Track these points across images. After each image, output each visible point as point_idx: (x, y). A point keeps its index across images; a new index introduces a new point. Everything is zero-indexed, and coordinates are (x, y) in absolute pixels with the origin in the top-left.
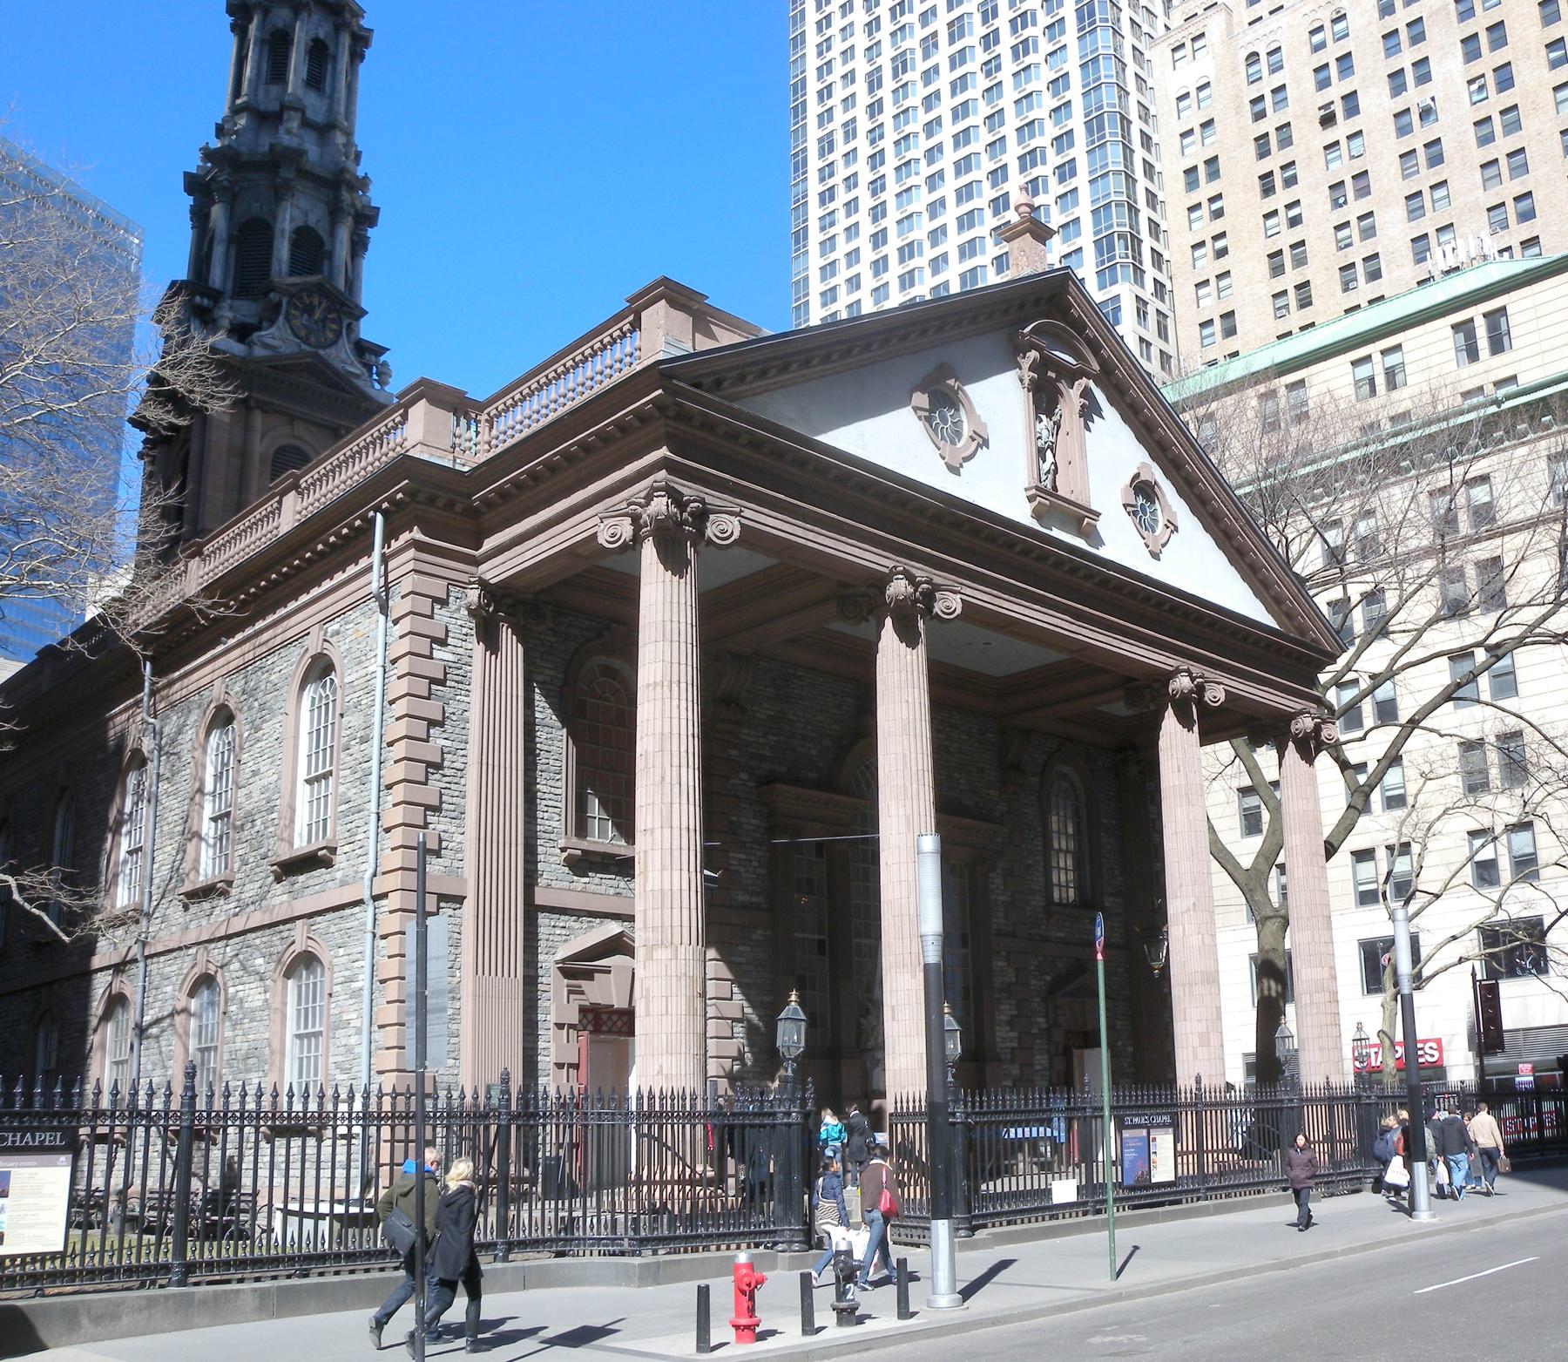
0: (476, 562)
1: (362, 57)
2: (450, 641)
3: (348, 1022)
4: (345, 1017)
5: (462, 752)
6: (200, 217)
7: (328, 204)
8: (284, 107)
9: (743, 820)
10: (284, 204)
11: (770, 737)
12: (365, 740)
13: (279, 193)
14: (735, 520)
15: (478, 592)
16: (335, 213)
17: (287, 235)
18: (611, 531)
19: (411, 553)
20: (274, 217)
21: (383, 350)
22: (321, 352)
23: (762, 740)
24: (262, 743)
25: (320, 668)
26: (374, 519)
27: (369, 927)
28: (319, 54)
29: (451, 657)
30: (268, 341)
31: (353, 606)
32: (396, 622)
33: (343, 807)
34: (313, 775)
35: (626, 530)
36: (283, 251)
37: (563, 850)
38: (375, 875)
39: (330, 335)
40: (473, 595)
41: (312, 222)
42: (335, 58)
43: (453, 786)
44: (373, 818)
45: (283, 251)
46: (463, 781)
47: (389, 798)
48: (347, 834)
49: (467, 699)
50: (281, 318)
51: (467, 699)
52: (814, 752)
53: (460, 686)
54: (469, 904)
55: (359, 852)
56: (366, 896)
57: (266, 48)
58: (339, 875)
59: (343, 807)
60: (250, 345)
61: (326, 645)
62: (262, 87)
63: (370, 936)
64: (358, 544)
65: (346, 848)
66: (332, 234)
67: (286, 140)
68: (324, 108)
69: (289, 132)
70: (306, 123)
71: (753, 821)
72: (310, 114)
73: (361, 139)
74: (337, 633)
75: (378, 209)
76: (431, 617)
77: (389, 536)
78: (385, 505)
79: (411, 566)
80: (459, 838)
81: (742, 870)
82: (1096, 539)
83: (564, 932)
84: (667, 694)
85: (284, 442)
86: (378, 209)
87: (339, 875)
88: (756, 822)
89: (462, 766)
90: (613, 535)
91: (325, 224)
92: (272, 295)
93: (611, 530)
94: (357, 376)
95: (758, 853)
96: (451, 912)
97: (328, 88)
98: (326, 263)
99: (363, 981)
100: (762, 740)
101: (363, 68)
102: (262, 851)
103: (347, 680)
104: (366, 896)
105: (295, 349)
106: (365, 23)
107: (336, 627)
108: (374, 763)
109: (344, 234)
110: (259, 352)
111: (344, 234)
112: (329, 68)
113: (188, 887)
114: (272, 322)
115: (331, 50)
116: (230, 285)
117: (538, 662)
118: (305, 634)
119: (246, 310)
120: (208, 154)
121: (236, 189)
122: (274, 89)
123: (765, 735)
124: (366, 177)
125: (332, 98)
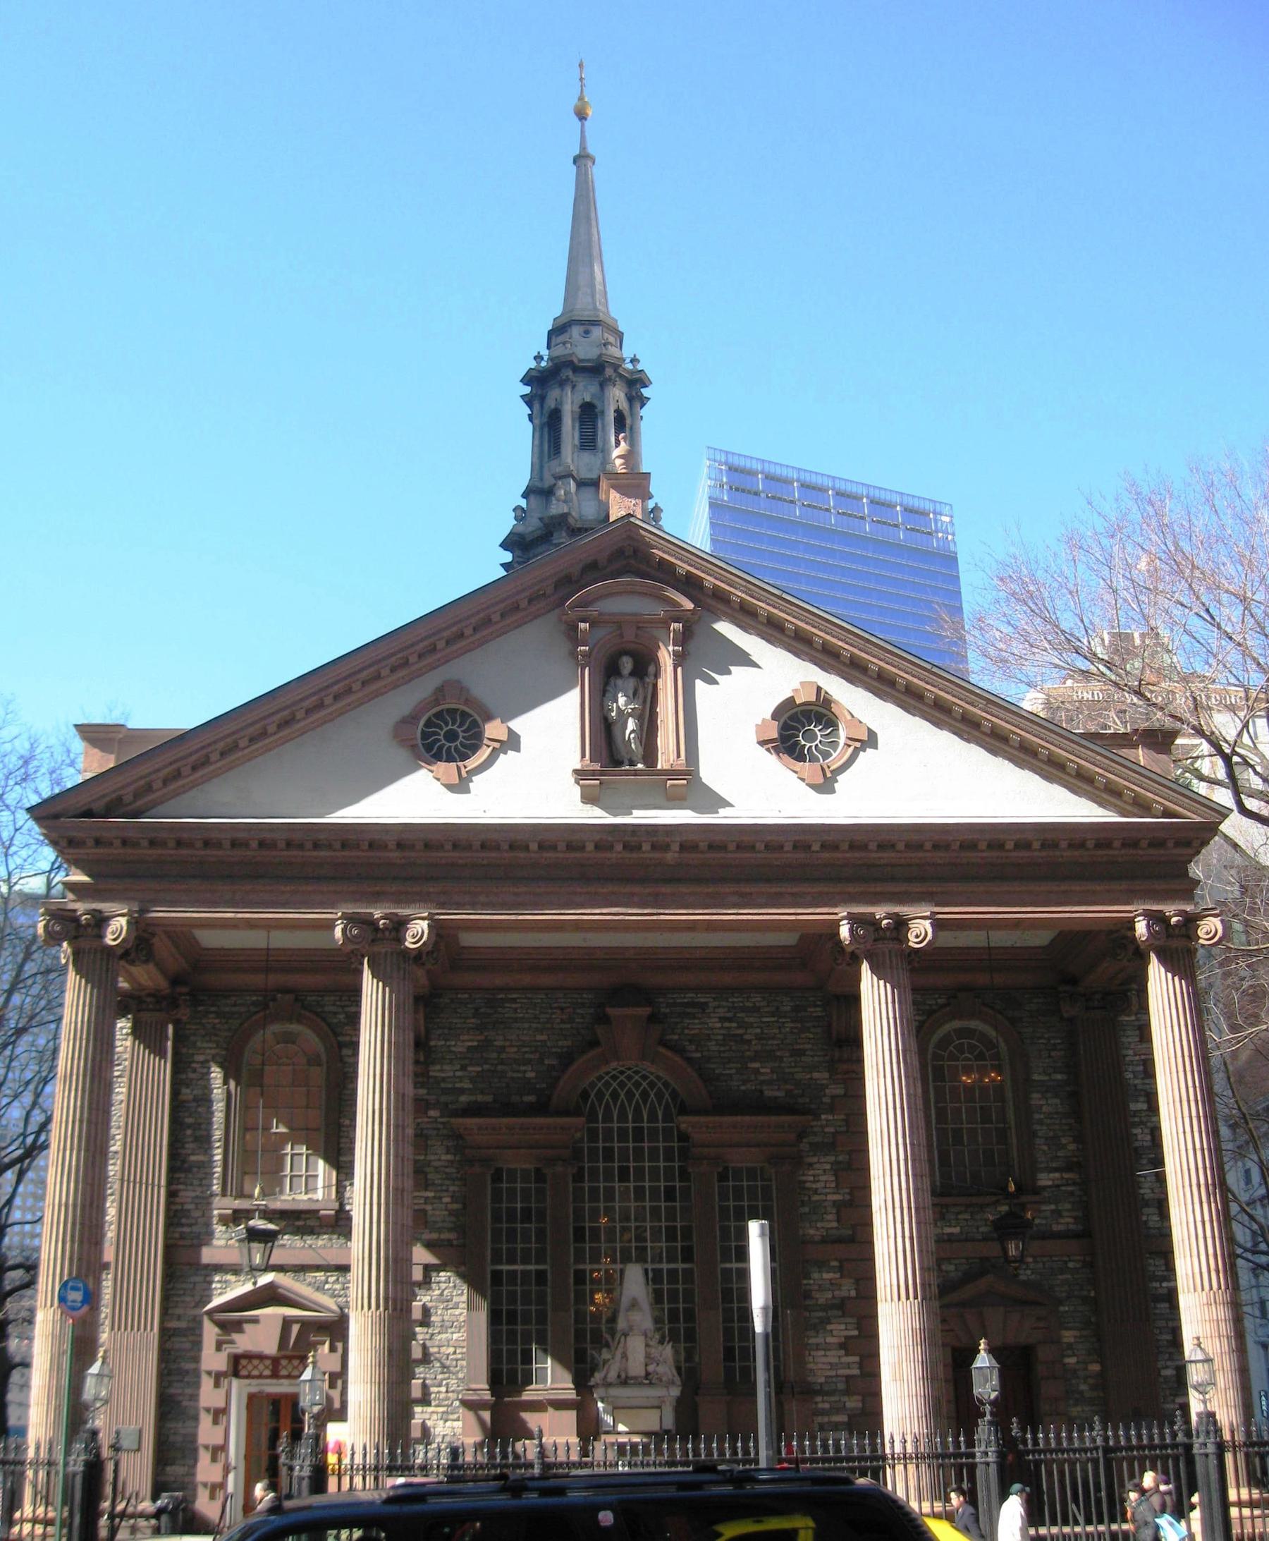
9: (432, 1158)
11: (470, 1069)
23: (458, 1074)
28: (589, 414)
52: (531, 1075)
57: (546, 430)
62: (546, 466)
71: (443, 1157)
81: (429, 1207)
82: (716, 802)
88: (449, 1157)
95: (452, 1188)
100: (458, 1074)
112: (600, 425)
117: (199, 1044)
123: (463, 1068)
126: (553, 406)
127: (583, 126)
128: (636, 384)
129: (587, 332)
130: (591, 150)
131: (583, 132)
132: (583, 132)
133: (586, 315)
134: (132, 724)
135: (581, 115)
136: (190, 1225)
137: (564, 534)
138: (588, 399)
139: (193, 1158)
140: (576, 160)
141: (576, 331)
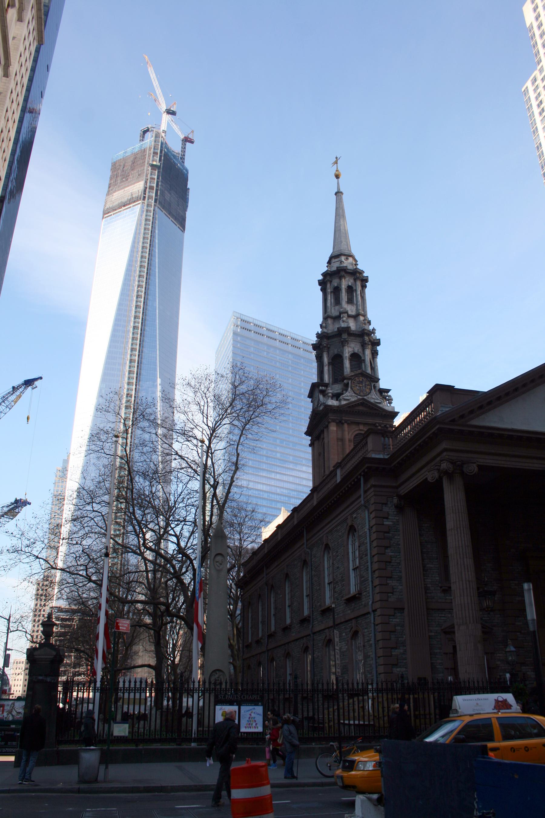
0: (397, 487)
1: (366, 287)
2: (390, 517)
3: (370, 656)
4: (369, 654)
5: (398, 557)
6: (319, 358)
7: (361, 343)
8: (341, 313)
10: (345, 347)
12: (366, 555)
13: (344, 343)
14: (475, 465)
15: (396, 500)
16: (363, 346)
17: (348, 358)
18: (431, 476)
19: (372, 489)
20: (343, 353)
21: (389, 390)
22: (365, 397)
24: (339, 557)
25: (352, 529)
26: (360, 478)
27: (372, 621)
28: (350, 290)
29: (391, 523)
30: (345, 398)
31: (359, 508)
32: (371, 513)
33: (363, 579)
34: (354, 567)
35: (436, 475)
36: (347, 364)
37: (441, 587)
38: (373, 602)
39: (368, 391)
40: (395, 500)
41: (356, 351)
42: (356, 290)
43: (397, 569)
44: (370, 583)
45: (347, 364)
46: (400, 567)
47: (375, 576)
48: (364, 589)
49: (399, 537)
50: (349, 389)
51: (399, 537)
53: (396, 533)
54: (406, 611)
55: (368, 595)
56: (370, 610)
57: (332, 294)
58: (363, 603)
59: (363, 579)
60: (340, 401)
61: (353, 522)
62: (333, 308)
63: (373, 625)
64: (356, 486)
65: (365, 594)
66: (364, 353)
67: (343, 325)
68: (355, 309)
69: (343, 321)
70: (349, 316)
72: (350, 313)
73: (370, 316)
74: (355, 518)
75: (380, 339)
76: (382, 510)
77: (366, 482)
78: (362, 474)
79: (373, 493)
80: (400, 587)
83: (444, 618)
84: (456, 532)
85: (357, 432)
86: (380, 339)
87: (363, 603)
89: (399, 562)
90: (432, 477)
91: (360, 350)
92: (345, 381)
93: (431, 476)
94: (380, 403)
96: (400, 614)
97: (355, 302)
98: (363, 364)
99: (372, 642)
101: (367, 290)
102: (342, 595)
103: (360, 534)
104: (370, 610)
105: (356, 399)
106: (365, 275)
107: (354, 516)
108: (369, 564)
109: (368, 352)
110: (344, 403)
111: (368, 352)
112: (354, 294)
113: (323, 608)
114: (347, 390)
115: (354, 288)
116: (331, 380)
118: (346, 519)
119: (337, 388)
120: (318, 336)
121: (329, 346)
122: (337, 307)
124: (374, 329)
125: (357, 304)
126: (336, 285)
127: (338, 181)
128: (365, 280)
129: (347, 259)
130: (341, 190)
131: (338, 183)
132: (338, 183)
133: (346, 252)
134: (457, 387)
135: (337, 177)
136: (431, 593)
137: (346, 335)
138: (350, 284)
139: (428, 566)
140: (336, 194)
141: (343, 258)
